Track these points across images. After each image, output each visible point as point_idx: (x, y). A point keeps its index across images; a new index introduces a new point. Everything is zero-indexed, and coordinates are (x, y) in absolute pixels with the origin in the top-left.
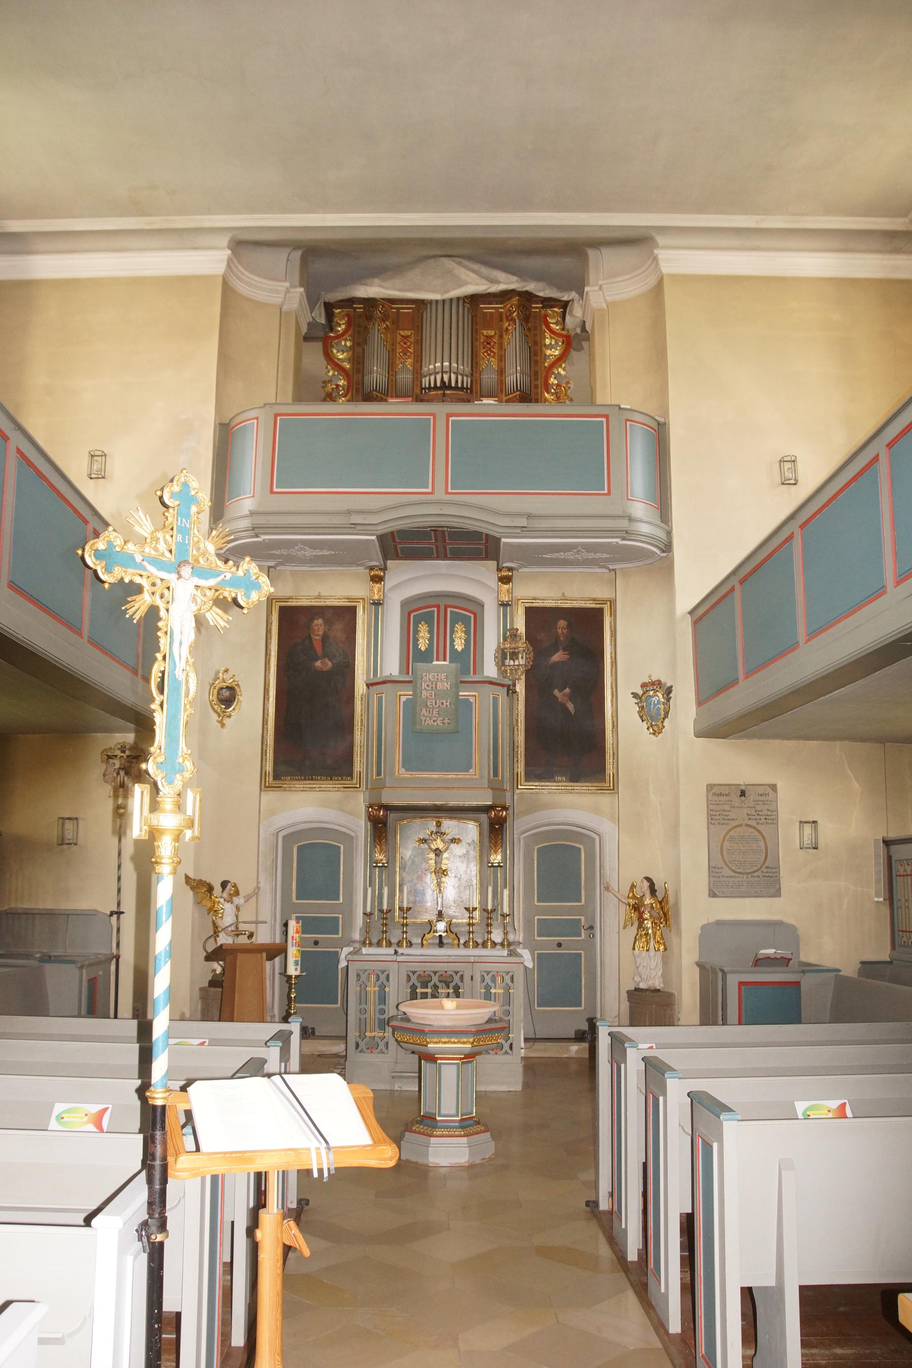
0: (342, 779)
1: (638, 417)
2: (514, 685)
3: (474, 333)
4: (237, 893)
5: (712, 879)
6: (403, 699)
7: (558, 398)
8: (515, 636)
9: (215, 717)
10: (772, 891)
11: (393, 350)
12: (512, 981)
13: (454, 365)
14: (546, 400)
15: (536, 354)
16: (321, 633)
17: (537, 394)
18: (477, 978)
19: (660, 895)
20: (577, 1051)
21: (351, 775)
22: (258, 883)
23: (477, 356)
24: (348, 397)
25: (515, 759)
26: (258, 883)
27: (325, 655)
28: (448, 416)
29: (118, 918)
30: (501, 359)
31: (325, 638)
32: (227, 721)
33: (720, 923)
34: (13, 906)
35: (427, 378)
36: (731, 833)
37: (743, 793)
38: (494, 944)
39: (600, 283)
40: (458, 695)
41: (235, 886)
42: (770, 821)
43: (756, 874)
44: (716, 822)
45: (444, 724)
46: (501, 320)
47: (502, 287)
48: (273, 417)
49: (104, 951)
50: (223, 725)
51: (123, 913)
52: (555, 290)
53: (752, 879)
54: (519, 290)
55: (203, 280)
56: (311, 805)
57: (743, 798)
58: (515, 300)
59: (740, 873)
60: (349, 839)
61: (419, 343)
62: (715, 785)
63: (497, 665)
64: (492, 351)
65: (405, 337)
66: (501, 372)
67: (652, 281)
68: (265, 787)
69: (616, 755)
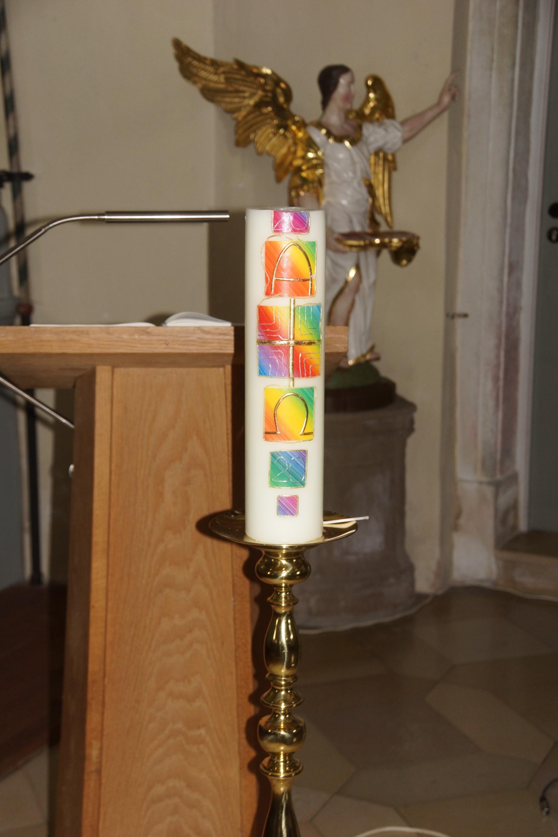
4: (386, 107)
29: (17, 193)
41: (377, 85)
51: (28, 177)
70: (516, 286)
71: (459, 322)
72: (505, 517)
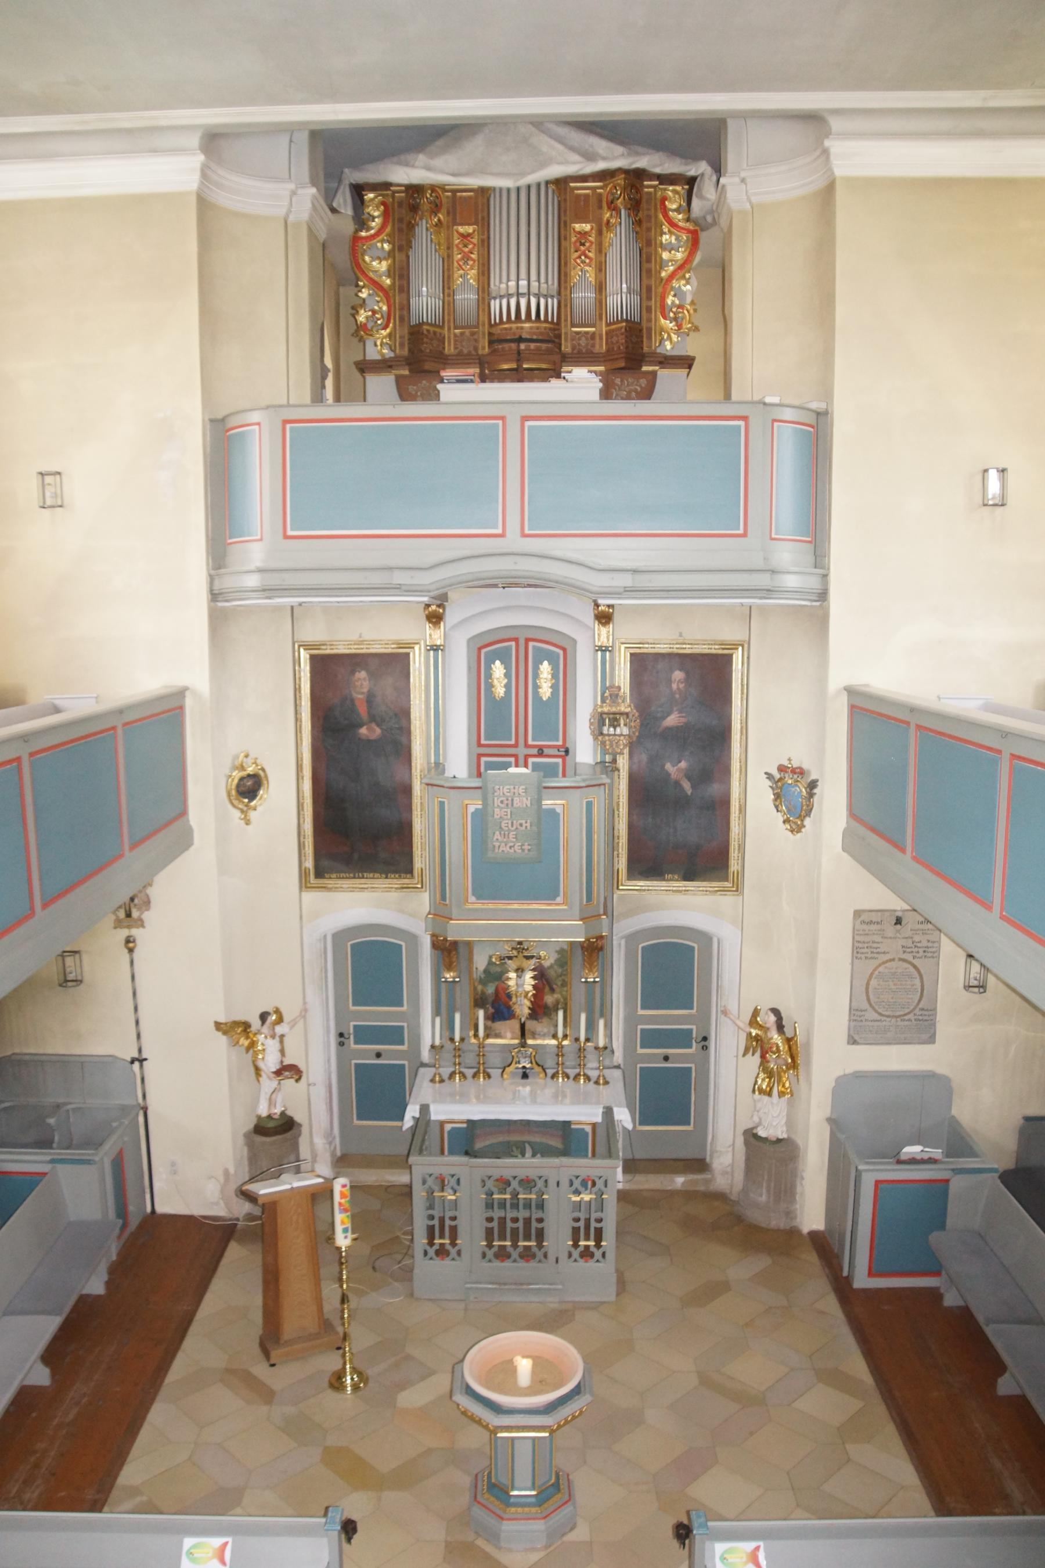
0: (400, 877)
1: (788, 414)
2: (614, 761)
3: (563, 226)
5: (853, 1024)
6: (471, 809)
7: (680, 327)
8: (617, 696)
9: (237, 814)
10: (925, 1037)
11: (449, 256)
12: (606, 1186)
13: (534, 284)
14: (662, 330)
15: (649, 261)
16: (365, 690)
17: (649, 320)
18: (565, 1183)
19: (789, 1034)
20: (683, 1184)
21: (409, 870)
22: (305, 1003)
23: (566, 264)
24: (388, 330)
25: (616, 853)
26: (305, 1003)
27: (373, 718)
28: (525, 419)
29: (141, 1066)
30: (601, 268)
31: (370, 698)
32: (252, 815)
33: (859, 1076)
34: (17, 1051)
35: (498, 301)
36: (881, 969)
37: (898, 921)
38: (588, 1078)
39: (743, 174)
40: (539, 804)
42: (930, 955)
43: (906, 1018)
44: (863, 956)
45: (523, 850)
46: (600, 207)
47: (601, 166)
48: (280, 427)
49: (129, 1101)
50: (248, 822)
51: (146, 1059)
52: (678, 160)
53: (902, 1023)
54: (626, 167)
55: (169, 199)
56: (363, 904)
57: (898, 926)
58: (620, 180)
59: (888, 1016)
60: (413, 939)
61: (485, 243)
62: (864, 911)
63: (593, 733)
64: (586, 256)
65: (465, 236)
66: (600, 288)
67: (815, 182)
68: (304, 884)
69: (742, 848)
70: (330, 1066)
71: (311, 1088)
72: (333, 1154)
